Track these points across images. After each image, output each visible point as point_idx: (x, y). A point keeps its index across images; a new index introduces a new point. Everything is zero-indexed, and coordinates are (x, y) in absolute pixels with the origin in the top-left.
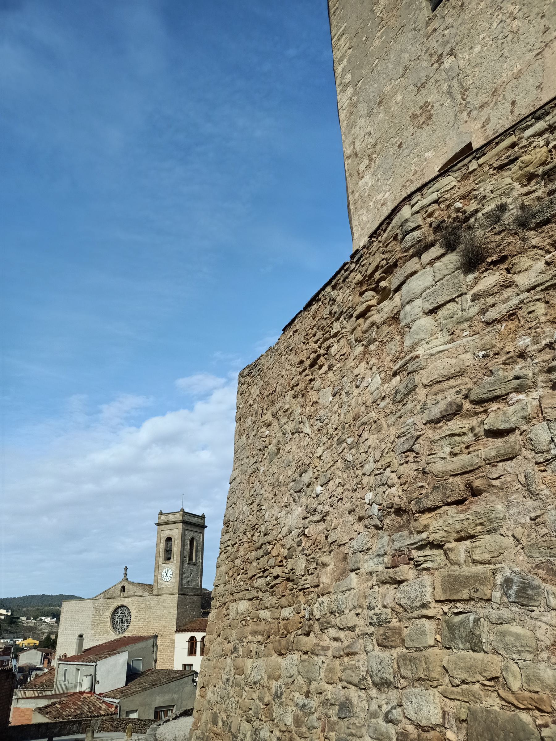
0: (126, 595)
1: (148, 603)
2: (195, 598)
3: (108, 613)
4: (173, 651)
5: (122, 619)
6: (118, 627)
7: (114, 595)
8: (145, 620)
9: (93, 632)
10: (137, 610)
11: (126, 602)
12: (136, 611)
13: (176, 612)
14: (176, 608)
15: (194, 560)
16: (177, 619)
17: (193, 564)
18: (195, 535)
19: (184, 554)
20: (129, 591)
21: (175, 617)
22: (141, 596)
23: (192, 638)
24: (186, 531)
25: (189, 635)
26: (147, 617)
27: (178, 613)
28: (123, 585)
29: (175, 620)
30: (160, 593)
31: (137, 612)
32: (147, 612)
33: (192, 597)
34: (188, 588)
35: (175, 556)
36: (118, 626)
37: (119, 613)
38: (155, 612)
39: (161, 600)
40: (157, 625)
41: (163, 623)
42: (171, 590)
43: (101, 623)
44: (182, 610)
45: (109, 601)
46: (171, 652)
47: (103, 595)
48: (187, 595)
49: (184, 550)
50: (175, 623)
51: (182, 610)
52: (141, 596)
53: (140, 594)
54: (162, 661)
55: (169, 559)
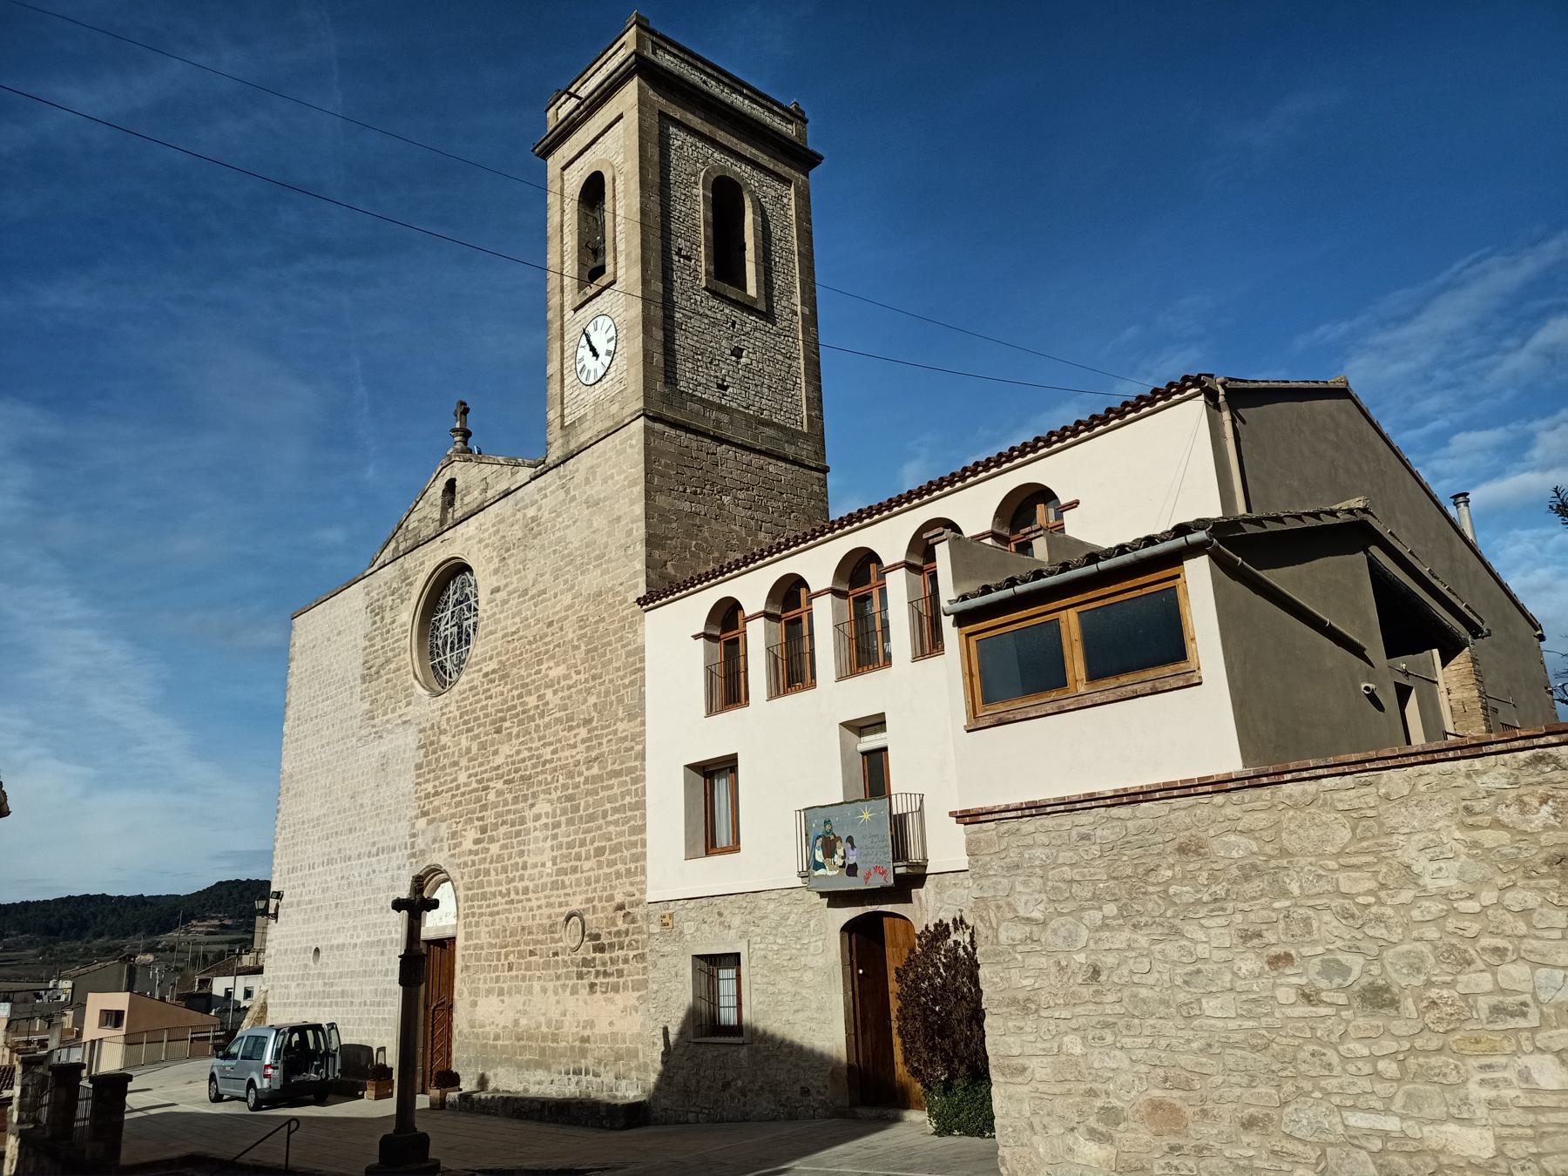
0: (458, 514)
1: (531, 512)
2: (775, 467)
3: (406, 615)
4: (637, 712)
5: (460, 627)
6: (448, 665)
7: (425, 533)
8: (525, 592)
9: (367, 706)
10: (496, 562)
11: (462, 543)
12: (492, 567)
13: (639, 509)
14: (639, 489)
15: (752, 290)
16: (652, 541)
17: (747, 307)
18: (742, 171)
19: (666, 234)
20: (467, 489)
21: (640, 531)
22: (507, 494)
23: (727, 615)
24: (678, 138)
25: (696, 607)
26: (531, 576)
27: (652, 512)
28: (447, 477)
29: (640, 549)
30: (573, 446)
31: (496, 571)
32: (530, 554)
33: (746, 457)
34: (721, 408)
35: (621, 246)
36: (449, 660)
37: (450, 604)
38: (558, 542)
39: (579, 477)
40: (567, 599)
41: (591, 581)
42: (615, 408)
43: (388, 661)
44: (686, 506)
45: (409, 562)
46: (631, 717)
47: (393, 545)
48: (720, 440)
49: (666, 215)
50: (639, 565)
51: (686, 506)
52: (507, 494)
53: (503, 486)
54: (595, 770)
55: (601, 270)
